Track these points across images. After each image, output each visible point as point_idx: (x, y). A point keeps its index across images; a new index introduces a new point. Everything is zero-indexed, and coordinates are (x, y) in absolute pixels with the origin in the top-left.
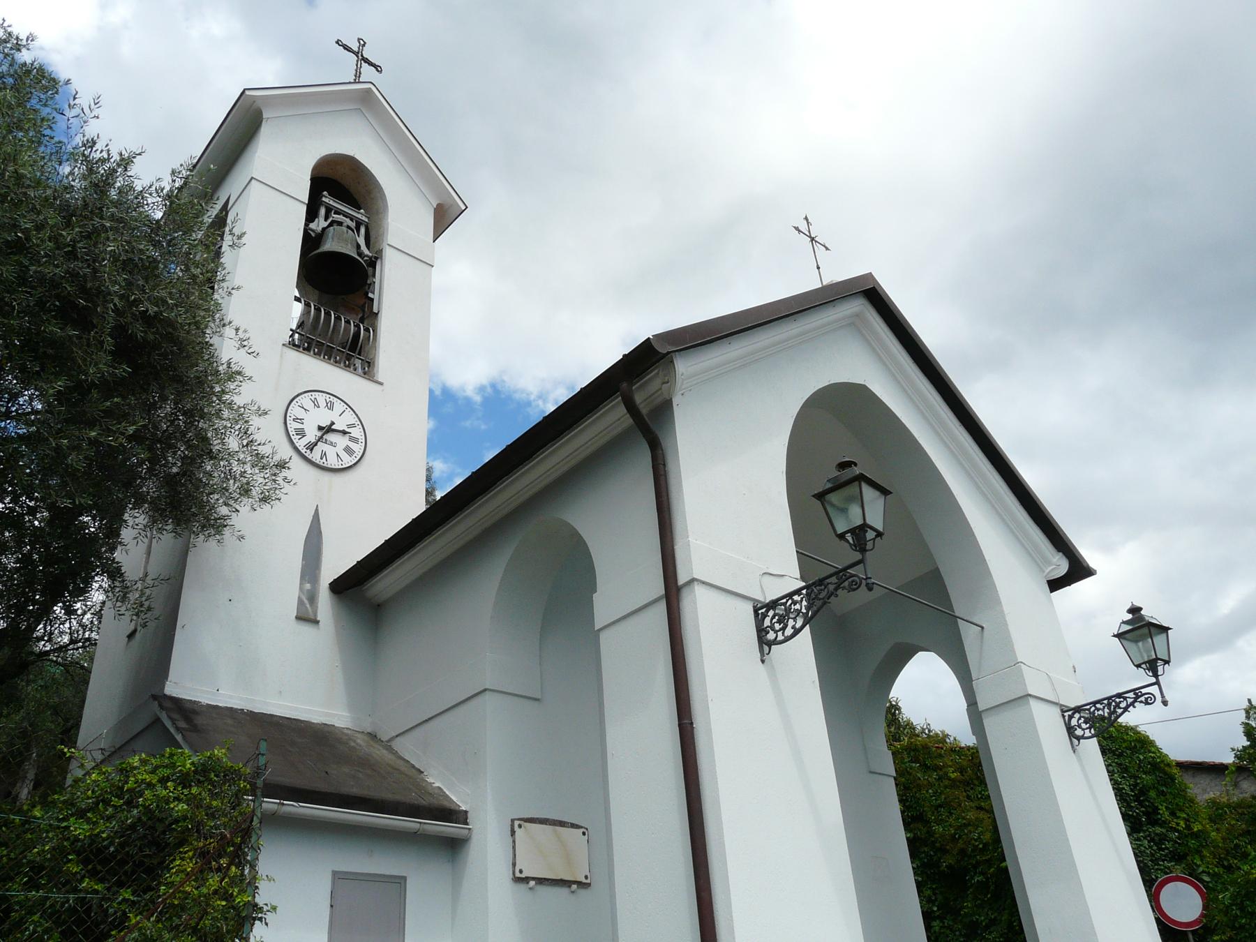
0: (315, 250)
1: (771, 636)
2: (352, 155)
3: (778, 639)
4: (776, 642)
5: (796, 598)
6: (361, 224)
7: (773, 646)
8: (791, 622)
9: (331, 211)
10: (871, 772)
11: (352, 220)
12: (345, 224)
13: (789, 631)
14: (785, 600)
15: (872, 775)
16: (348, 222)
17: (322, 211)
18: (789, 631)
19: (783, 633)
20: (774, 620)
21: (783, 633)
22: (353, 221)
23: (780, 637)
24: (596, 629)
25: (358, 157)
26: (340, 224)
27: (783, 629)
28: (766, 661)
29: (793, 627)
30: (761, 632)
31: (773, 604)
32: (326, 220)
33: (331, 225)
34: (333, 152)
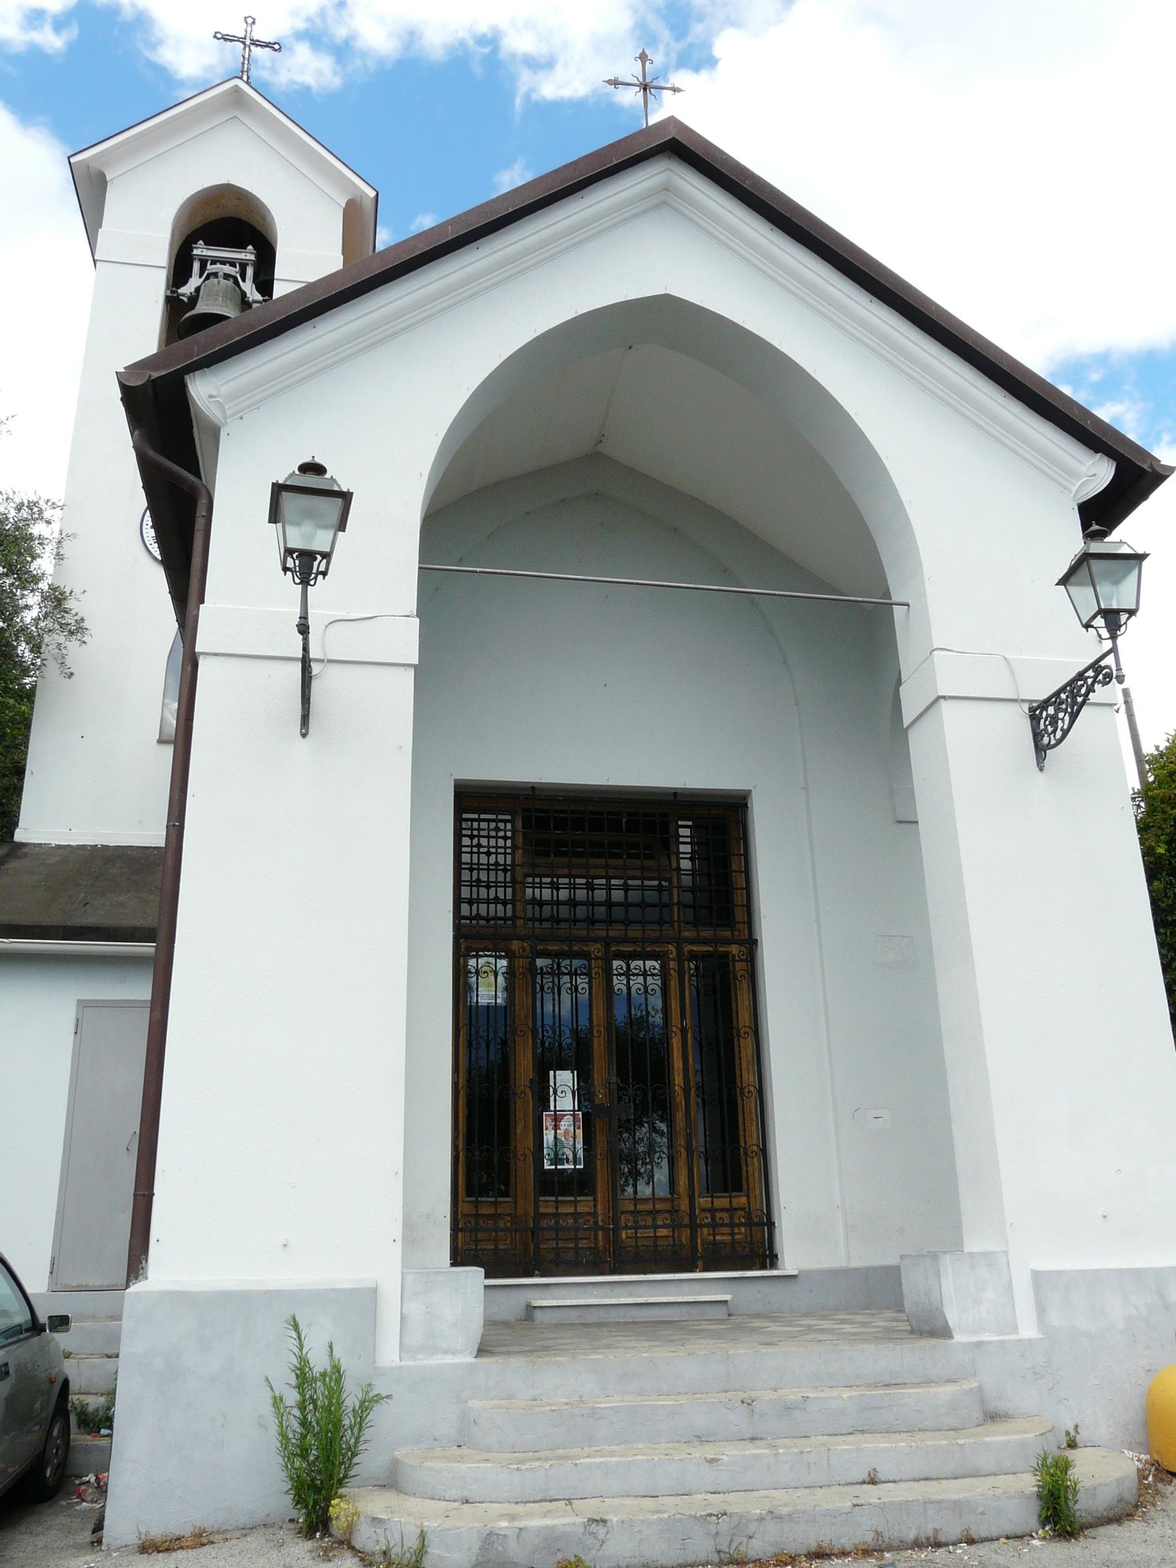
0: (191, 310)
1: (1046, 740)
2: (226, 182)
3: (1052, 743)
4: (1050, 746)
5: (1063, 696)
6: (247, 264)
7: (1048, 751)
8: (1060, 724)
9: (207, 264)
10: (900, 822)
11: (233, 265)
12: (221, 274)
13: (1059, 734)
14: (1054, 699)
15: (900, 825)
16: (228, 269)
17: (196, 266)
18: (1059, 734)
19: (1054, 736)
20: (1047, 723)
21: (1054, 736)
22: (236, 267)
23: (1053, 742)
24: (905, 727)
25: (233, 182)
26: (215, 275)
27: (1054, 732)
28: (1045, 768)
29: (1062, 729)
30: (1037, 735)
31: (1045, 704)
32: (200, 277)
33: (207, 278)
34: (201, 188)
